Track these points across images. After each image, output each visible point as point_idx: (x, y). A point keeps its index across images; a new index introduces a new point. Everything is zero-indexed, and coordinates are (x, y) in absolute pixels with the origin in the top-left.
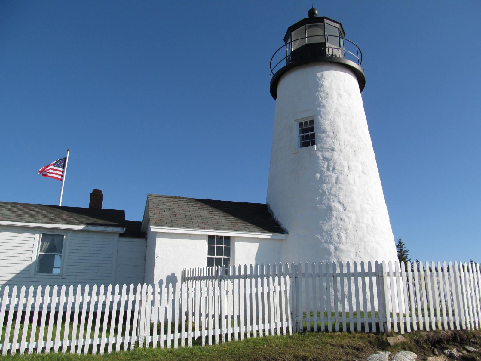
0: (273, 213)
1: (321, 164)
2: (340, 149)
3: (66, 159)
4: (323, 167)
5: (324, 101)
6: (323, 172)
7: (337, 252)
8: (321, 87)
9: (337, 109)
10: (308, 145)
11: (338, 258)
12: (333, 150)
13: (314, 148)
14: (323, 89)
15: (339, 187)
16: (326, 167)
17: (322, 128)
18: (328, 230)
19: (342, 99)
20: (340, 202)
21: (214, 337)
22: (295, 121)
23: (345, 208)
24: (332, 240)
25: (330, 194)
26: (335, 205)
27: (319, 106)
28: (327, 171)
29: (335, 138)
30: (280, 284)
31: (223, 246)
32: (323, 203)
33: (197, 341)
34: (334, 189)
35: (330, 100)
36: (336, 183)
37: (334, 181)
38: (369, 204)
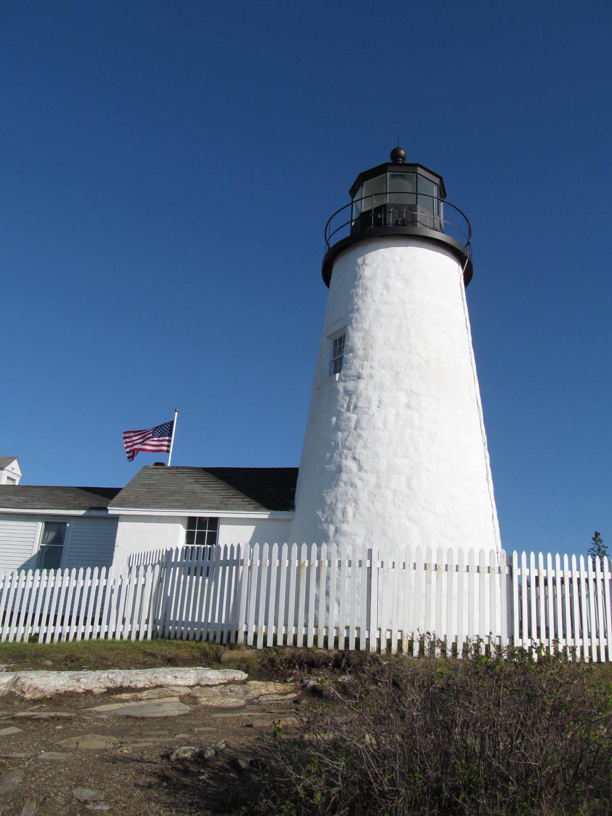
1: (339, 402)
2: (370, 374)
3: (172, 422)
4: (342, 406)
5: (360, 302)
6: (341, 414)
7: (338, 535)
8: (360, 279)
9: (377, 310)
12: (359, 377)
13: (335, 377)
14: (362, 283)
15: (358, 434)
16: (345, 406)
17: (349, 344)
18: (332, 503)
19: (390, 292)
20: (354, 459)
21: (53, 635)
22: (328, 338)
23: (361, 467)
24: (334, 517)
25: (344, 446)
26: (350, 464)
28: (346, 411)
29: (366, 358)
30: (137, 576)
31: (207, 531)
32: (333, 461)
33: (34, 638)
34: (350, 439)
35: (368, 299)
36: (355, 429)
37: (353, 426)
38: (407, 457)
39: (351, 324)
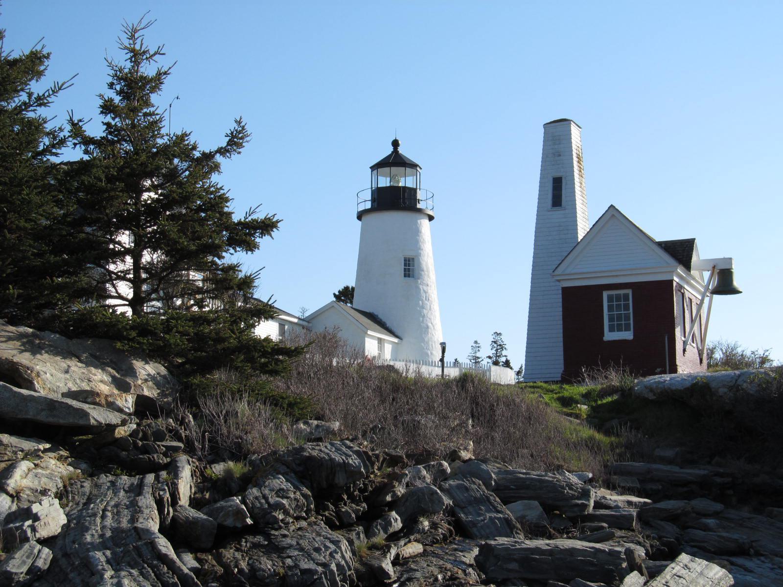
0: (384, 322)
10: (409, 276)
11: (432, 359)
12: (428, 285)
25: (427, 317)
26: (430, 325)
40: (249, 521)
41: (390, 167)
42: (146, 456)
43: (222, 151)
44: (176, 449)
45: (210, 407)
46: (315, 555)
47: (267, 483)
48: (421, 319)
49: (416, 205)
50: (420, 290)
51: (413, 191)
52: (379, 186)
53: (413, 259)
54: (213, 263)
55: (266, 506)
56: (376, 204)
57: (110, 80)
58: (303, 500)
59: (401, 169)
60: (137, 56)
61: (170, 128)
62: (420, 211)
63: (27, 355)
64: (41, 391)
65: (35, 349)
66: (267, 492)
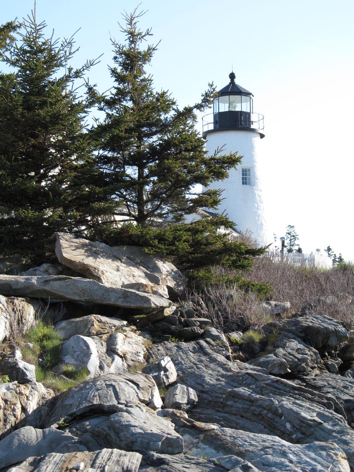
10: (246, 184)
26: (263, 222)
27: (254, 161)
39: (255, 167)
40: (290, 371)
41: (229, 95)
42: (190, 328)
43: (199, 107)
44: (206, 323)
45: (213, 294)
46: (345, 390)
47: (287, 345)
48: (257, 218)
49: (250, 126)
50: (256, 194)
51: (249, 114)
52: (220, 111)
53: (249, 170)
54: (78, 173)
55: (296, 360)
56: (218, 125)
57: (114, 54)
58: (314, 357)
59: (238, 97)
60: (133, 37)
61: (156, 88)
62: (253, 130)
63: (91, 259)
64: (106, 283)
65: (95, 255)
66: (290, 351)
